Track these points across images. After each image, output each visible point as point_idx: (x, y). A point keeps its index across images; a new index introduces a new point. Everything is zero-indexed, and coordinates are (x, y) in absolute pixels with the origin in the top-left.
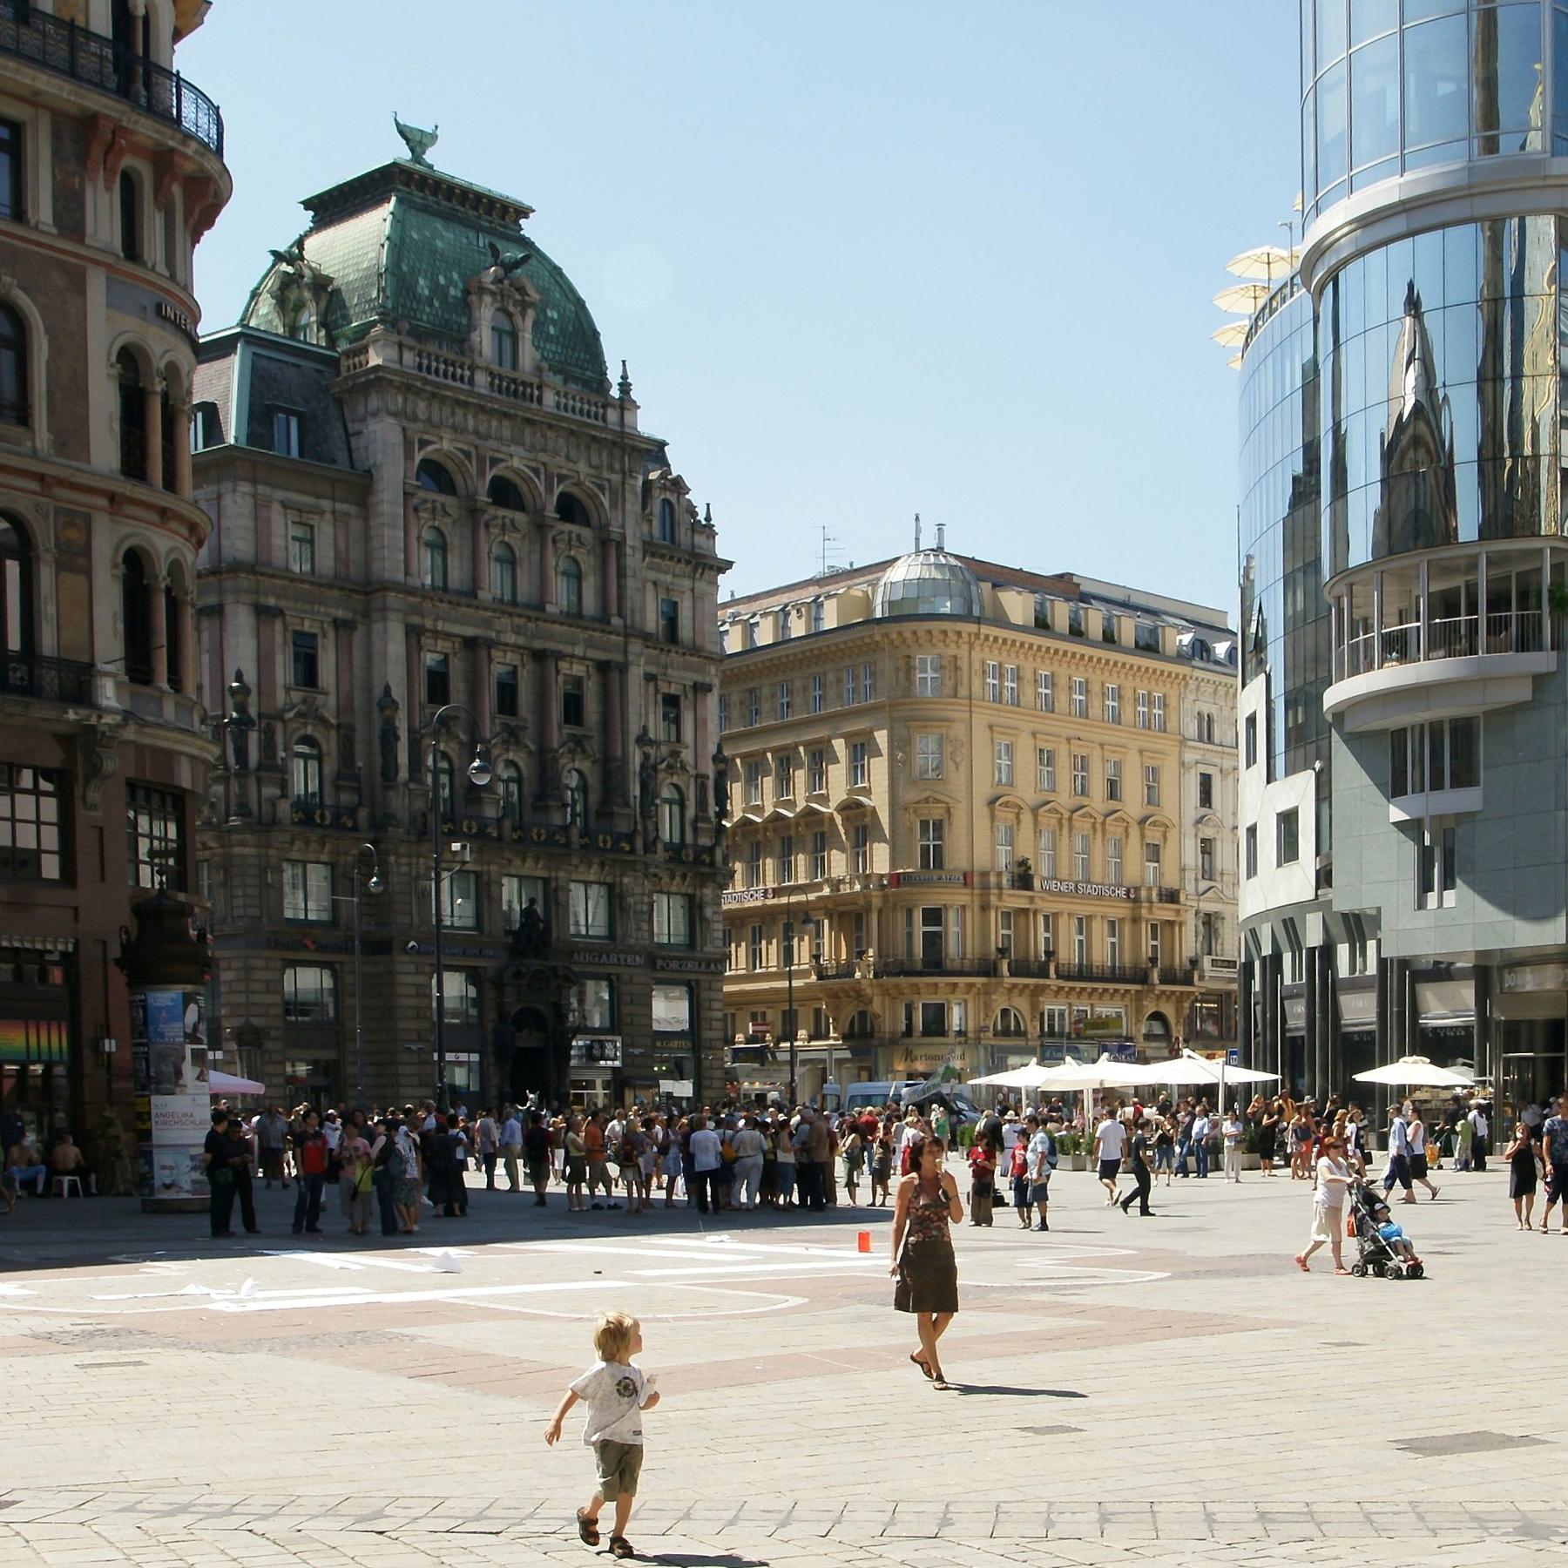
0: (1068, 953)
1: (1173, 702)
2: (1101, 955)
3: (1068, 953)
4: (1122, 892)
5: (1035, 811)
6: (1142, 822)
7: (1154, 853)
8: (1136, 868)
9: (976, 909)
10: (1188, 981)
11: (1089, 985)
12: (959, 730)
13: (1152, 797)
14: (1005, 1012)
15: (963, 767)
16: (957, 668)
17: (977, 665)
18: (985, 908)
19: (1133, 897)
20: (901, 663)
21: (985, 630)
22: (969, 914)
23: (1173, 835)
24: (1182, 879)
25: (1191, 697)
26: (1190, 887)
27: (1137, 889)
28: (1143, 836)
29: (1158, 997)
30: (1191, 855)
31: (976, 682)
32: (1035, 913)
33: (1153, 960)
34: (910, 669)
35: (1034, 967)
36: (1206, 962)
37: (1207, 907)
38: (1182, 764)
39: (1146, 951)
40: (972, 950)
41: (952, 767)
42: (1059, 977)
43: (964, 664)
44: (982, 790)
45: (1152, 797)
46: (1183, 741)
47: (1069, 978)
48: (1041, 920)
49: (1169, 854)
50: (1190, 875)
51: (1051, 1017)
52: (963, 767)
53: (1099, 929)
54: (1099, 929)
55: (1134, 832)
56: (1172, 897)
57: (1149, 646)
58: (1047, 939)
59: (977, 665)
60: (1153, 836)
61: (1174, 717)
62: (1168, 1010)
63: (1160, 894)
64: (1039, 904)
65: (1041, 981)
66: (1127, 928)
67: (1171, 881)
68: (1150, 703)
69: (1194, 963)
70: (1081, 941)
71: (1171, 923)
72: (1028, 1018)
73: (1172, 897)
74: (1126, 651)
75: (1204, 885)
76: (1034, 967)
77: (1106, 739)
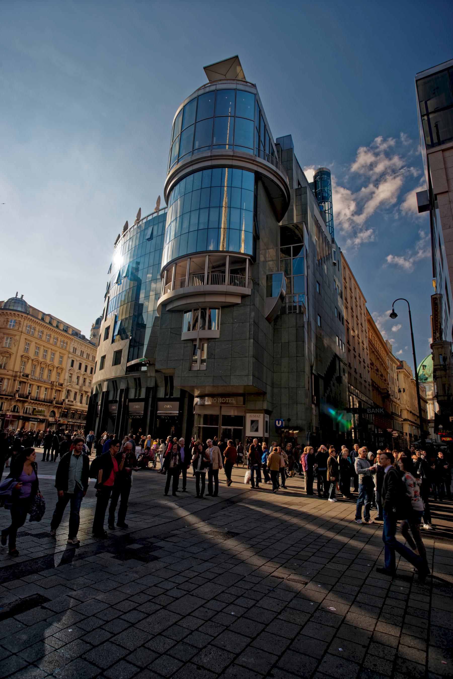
0: (34, 394)
1: (69, 344)
2: (42, 396)
3: (34, 394)
4: (50, 382)
5: (32, 360)
6: (57, 368)
7: (59, 374)
8: (54, 378)
9: (13, 380)
10: (62, 404)
11: (38, 402)
12: (17, 338)
13: (61, 362)
14: (15, 406)
15: (16, 346)
16: (20, 324)
17: (25, 324)
18: (15, 380)
19: (52, 384)
20: (6, 320)
21: (29, 316)
22: (10, 381)
23: (64, 371)
24: (64, 382)
25: (73, 343)
26: (66, 384)
27: (54, 382)
28: (57, 371)
29: (54, 407)
30: (67, 377)
31: (24, 328)
32: (28, 383)
33: (55, 398)
34: (8, 321)
35: (25, 396)
36: (67, 400)
37: (68, 388)
38: (68, 357)
39: (53, 397)
40: (9, 390)
41: (14, 346)
42: (31, 399)
43: (22, 323)
44: (21, 352)
45: (61, 362)
46: (69, 352)
47: (33, 400)
48: (29, 385)
49: (62, 376)
50: (66, 381)
51: (27, 408)
52: (16, 346)
53: (43, 389)
54: (43, 389)
55: (55, 369)
56: (61, 385)
57: (66, 331)
58: (29, 390)
59: (25, 324)
60: (59, 371)
61: (68, 347)
62: (56, 410)
63: (59, 384)
64: (29, 381)
65: (26, 400)
66: (50, 390)
67: (61, 382)
68: (64, 343)
69: (64, 400)
70: (38, 392)
71: (60, 391)
72: (21, 408)
73: (61, 385)
74: (61, 330)
75: (69, 384)
76: (25, 396)
77: (52, 348)
